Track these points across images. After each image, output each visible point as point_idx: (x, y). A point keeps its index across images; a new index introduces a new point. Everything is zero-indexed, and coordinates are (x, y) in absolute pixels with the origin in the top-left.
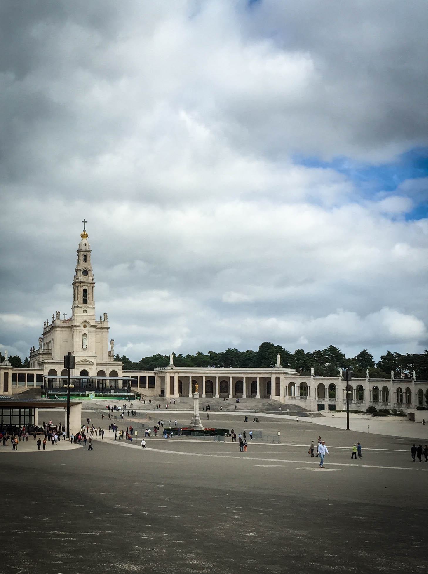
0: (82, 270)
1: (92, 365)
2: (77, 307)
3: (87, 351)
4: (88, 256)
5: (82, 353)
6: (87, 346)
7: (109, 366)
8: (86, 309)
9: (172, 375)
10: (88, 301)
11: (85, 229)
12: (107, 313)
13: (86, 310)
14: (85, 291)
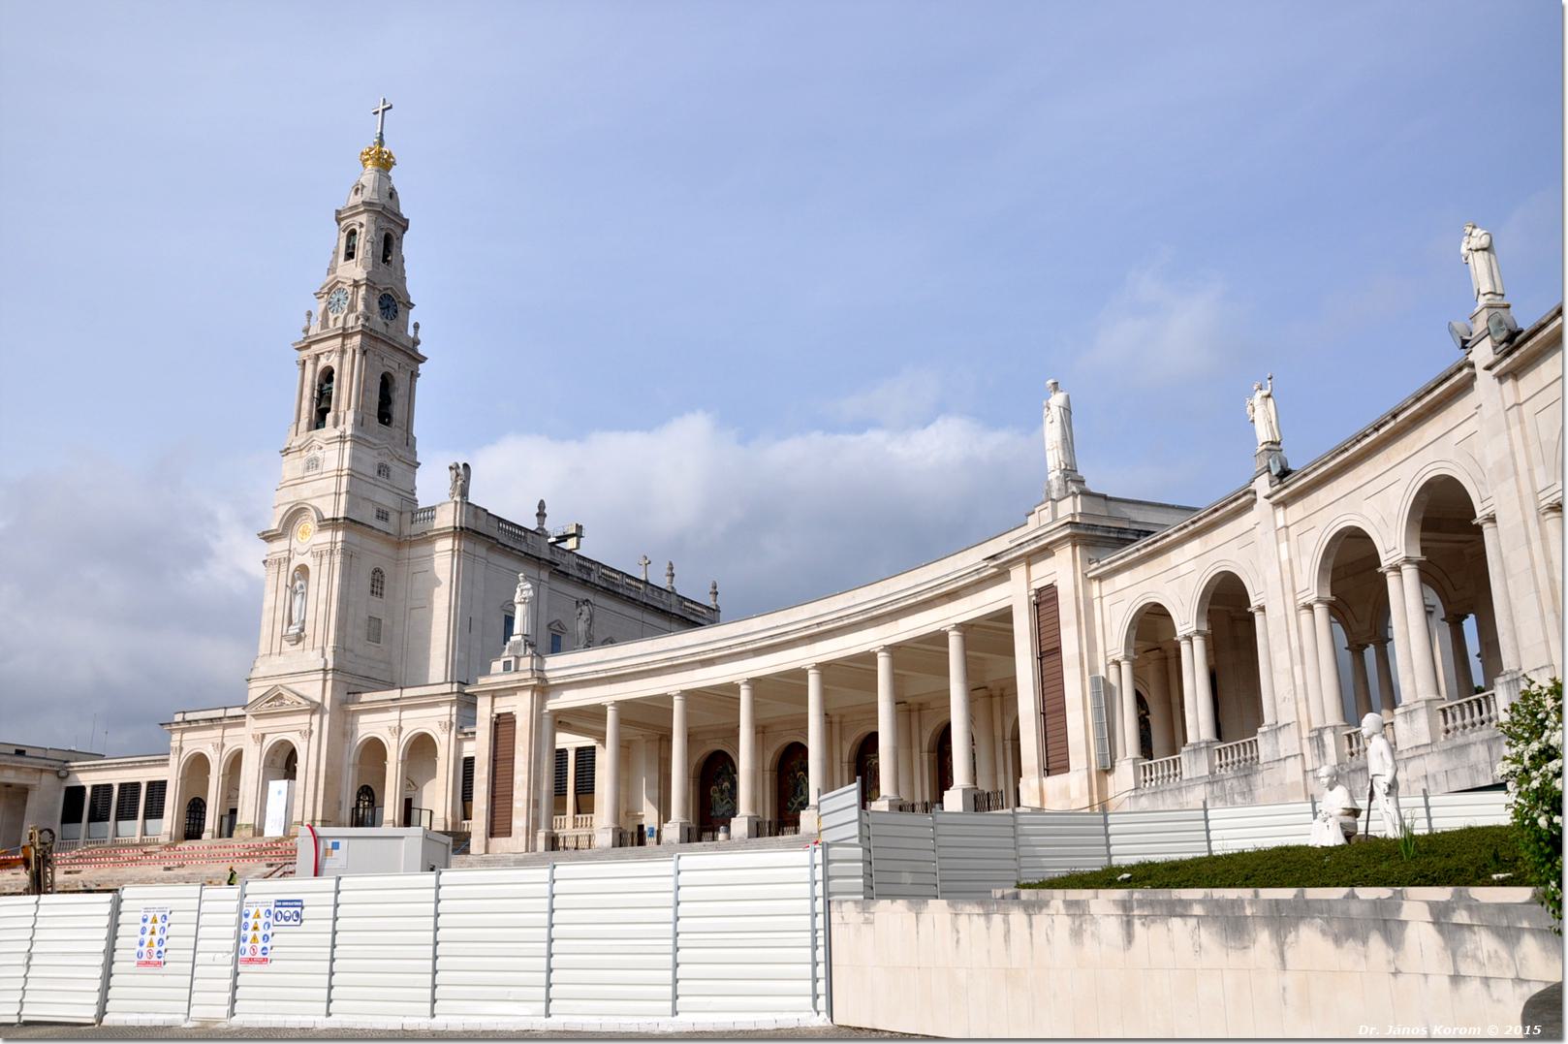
0: (326, 290)
1: (313, 712)
2: (286, 452)
3: (301, 644)
4: (364, 230)
5: (277, 660)
6: (304, 621)
7: (402, 708)
8: (319, 454)
9: (503, 705)
10: (330, 417)
11: (381, 134)
12: (466, 466)
13: (316, 459)
14: (328, 375)
